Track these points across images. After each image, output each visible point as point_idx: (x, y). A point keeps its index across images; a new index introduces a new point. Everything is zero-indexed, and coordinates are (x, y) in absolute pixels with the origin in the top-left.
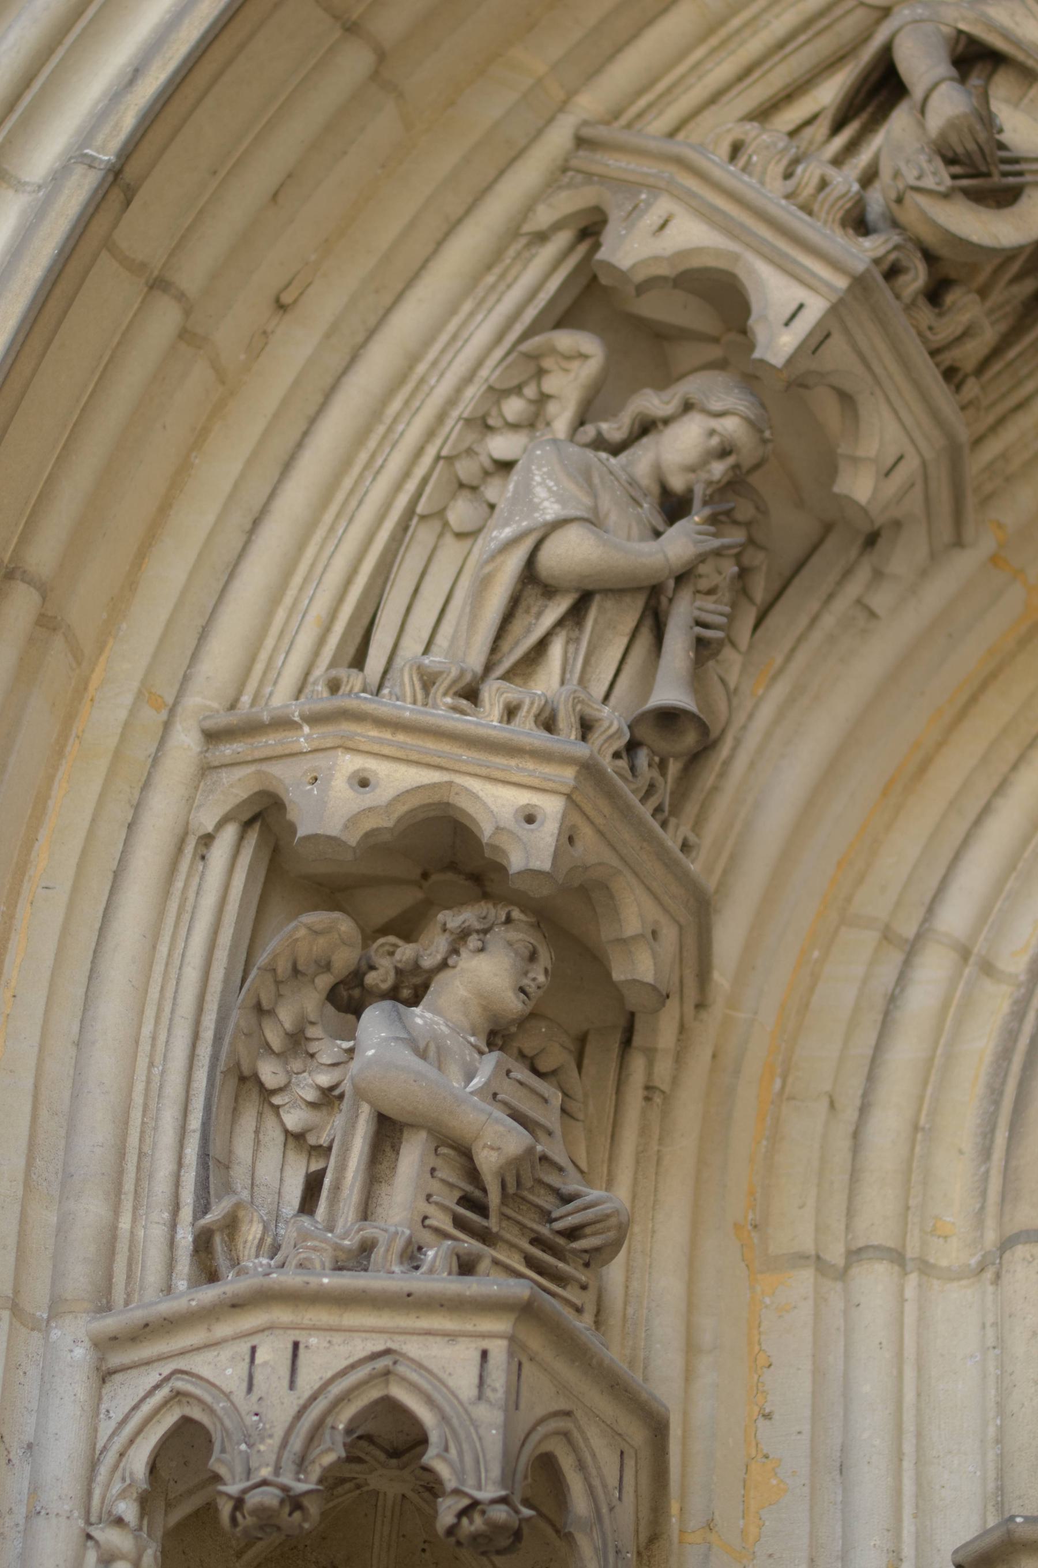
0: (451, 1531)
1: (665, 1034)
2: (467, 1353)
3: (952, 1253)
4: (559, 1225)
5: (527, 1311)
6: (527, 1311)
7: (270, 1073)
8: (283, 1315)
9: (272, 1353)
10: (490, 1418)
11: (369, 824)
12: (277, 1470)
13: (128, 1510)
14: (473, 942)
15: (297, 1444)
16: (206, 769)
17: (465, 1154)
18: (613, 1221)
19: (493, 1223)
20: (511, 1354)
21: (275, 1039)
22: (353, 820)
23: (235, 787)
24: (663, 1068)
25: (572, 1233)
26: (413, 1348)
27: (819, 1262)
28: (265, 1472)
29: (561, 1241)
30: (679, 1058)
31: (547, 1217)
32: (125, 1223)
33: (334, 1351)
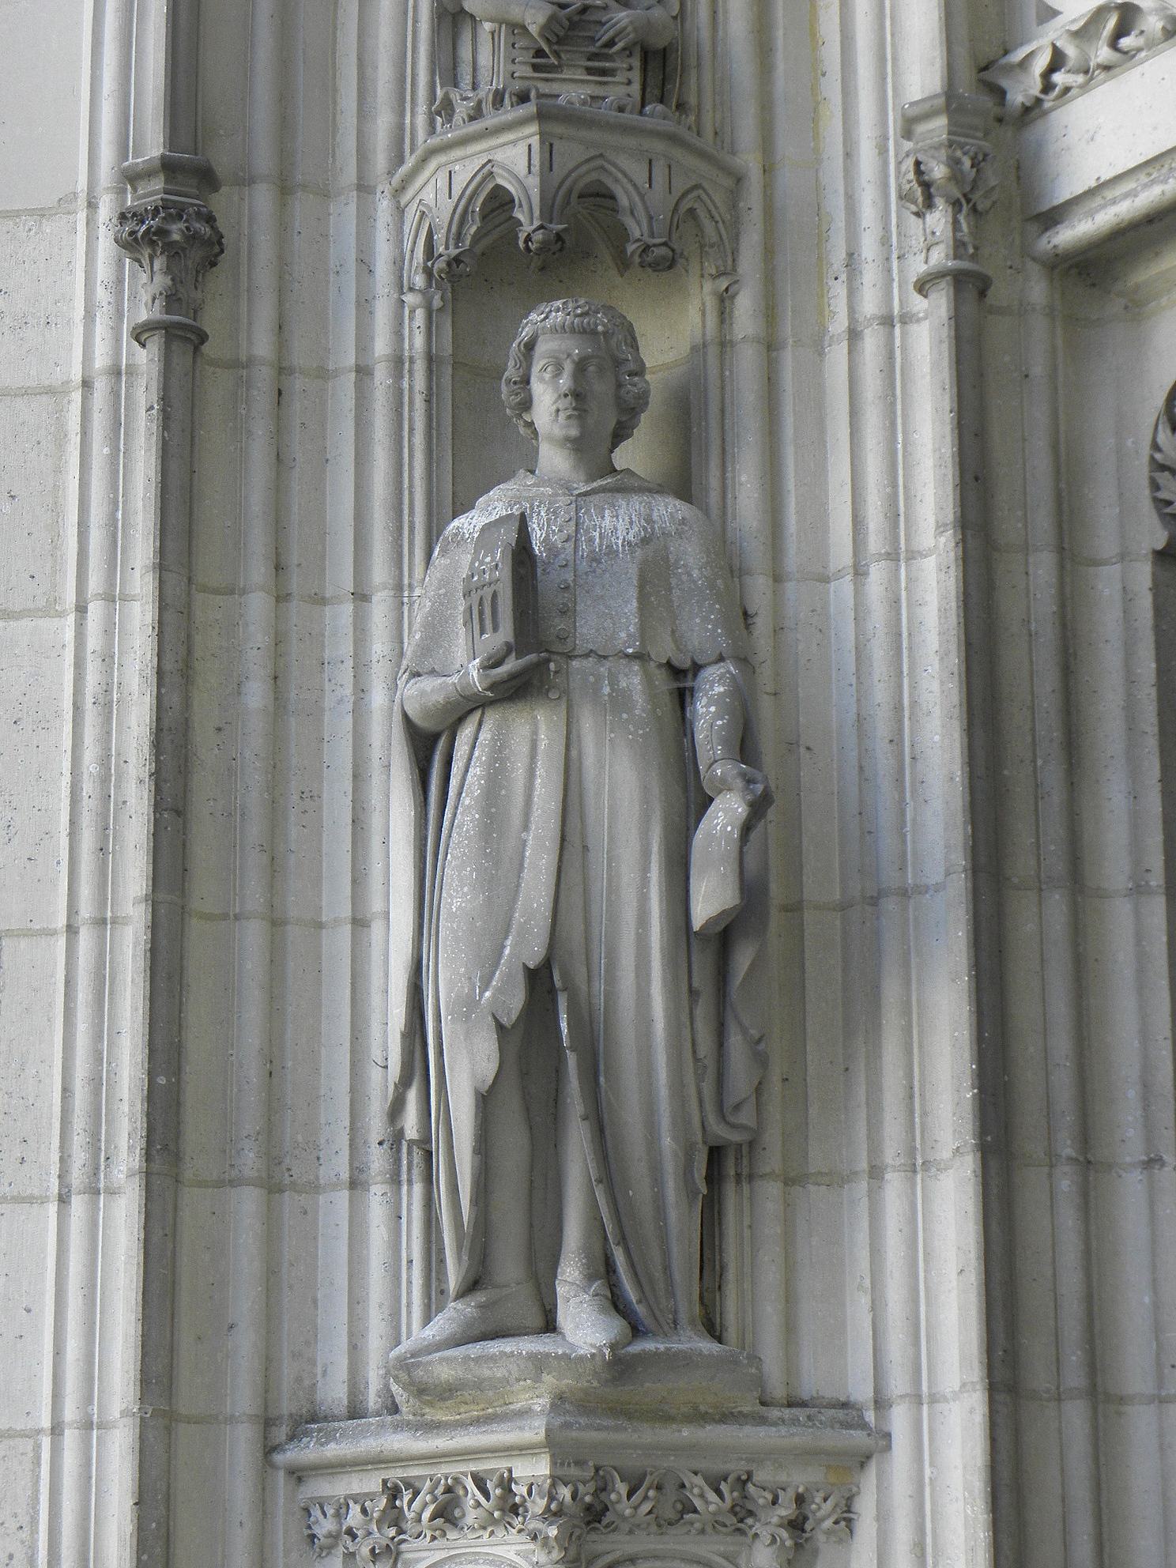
0: (528, 249)
2: (522, 149)
4: (599, 44)
8: (442, 159)
10: (533, 183)
12: (447, 248)
18: (630, 29)
19: (553, 60)
20: (542, 142)
29: (606, 51)
32: (408, 121)
33: (465, 169)
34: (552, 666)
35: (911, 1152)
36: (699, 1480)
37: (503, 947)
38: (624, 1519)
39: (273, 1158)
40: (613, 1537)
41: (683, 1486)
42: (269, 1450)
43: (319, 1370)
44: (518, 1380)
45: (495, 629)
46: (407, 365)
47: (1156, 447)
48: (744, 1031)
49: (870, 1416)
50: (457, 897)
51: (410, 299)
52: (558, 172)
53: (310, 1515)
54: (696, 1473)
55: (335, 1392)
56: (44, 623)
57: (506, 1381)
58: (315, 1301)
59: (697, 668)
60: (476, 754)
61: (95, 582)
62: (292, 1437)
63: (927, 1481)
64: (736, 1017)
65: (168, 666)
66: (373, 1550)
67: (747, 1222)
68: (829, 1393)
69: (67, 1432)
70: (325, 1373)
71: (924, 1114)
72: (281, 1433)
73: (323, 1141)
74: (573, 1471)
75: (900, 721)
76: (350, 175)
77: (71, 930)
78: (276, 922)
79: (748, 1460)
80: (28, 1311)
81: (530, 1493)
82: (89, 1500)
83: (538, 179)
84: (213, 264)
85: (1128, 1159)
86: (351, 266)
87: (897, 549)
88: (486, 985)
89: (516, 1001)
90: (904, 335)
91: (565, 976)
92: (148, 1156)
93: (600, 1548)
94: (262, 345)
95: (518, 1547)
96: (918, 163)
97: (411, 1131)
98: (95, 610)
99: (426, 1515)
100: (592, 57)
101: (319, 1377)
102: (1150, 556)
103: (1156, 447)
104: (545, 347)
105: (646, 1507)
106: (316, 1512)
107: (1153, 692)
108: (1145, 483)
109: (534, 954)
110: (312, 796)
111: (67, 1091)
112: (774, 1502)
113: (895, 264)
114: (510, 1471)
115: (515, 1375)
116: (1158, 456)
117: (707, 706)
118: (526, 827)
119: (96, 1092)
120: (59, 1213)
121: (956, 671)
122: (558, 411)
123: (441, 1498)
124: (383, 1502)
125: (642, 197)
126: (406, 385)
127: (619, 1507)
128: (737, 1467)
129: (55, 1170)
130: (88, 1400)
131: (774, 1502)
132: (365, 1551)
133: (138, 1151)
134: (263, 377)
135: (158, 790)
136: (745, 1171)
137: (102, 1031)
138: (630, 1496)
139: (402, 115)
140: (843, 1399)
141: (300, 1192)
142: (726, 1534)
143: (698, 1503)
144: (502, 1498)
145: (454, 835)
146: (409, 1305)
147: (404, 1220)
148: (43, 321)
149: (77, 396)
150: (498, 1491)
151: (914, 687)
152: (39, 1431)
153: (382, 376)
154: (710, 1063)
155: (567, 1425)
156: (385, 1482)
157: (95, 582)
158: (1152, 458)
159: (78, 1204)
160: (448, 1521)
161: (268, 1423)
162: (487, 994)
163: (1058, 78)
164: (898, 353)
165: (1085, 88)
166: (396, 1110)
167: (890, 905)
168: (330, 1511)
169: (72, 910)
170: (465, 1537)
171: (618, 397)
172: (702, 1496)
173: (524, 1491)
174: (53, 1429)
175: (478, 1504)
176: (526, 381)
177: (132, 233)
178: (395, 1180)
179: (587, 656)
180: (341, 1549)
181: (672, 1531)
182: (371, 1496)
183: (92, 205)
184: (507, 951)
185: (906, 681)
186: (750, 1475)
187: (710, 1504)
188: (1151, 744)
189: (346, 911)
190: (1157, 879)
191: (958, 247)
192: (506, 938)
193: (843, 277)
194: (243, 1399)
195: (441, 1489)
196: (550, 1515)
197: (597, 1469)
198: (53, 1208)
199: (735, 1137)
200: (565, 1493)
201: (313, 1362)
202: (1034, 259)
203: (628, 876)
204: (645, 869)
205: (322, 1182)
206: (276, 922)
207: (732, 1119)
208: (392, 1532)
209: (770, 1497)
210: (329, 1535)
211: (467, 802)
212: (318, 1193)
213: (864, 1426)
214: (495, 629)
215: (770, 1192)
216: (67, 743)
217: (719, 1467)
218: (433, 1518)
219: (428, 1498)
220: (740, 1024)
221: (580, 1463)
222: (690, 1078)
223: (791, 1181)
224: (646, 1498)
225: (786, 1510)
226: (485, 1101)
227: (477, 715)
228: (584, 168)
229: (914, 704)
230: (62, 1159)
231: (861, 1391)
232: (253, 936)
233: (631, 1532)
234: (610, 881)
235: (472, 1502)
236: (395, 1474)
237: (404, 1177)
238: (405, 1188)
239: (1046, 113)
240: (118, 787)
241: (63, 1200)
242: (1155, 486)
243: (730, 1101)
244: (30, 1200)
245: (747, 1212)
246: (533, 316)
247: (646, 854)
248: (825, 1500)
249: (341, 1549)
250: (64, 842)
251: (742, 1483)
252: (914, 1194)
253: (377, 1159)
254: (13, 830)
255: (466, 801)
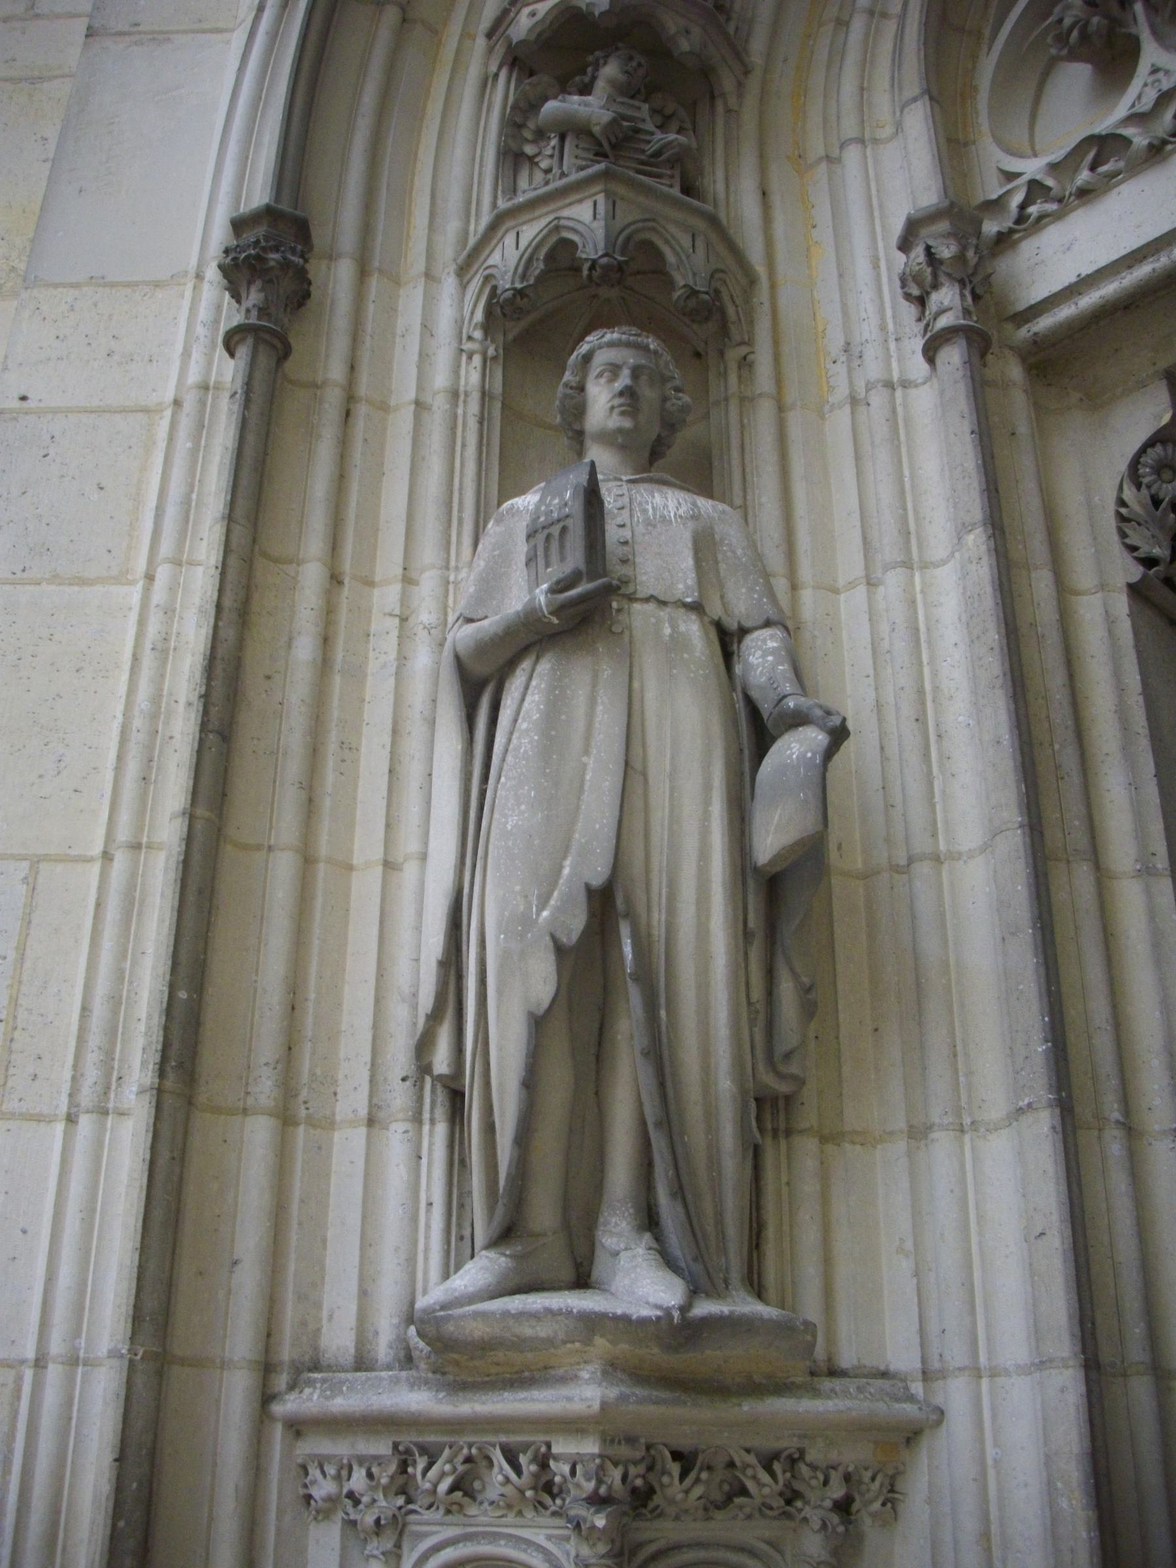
0: (590, 276)
1: (727, 83)
3: (888, 131)
5: (606, 175)
6: (606, 175)
7: (529, 150)
8: (509, 224)
9: (510, 240)
11: (538, 30)
12: (513, 283)
13: (478, 334)
14: (602, 61)
15: (520, 270)
16: (490, 50)
17: (590, 134)
20: (607, 197)
21: (528, 134)
22: (530, 30)
23: (500, 50)
24: (733, 102)
25: (658, 154)
26: (566, 213)
27: (828, 158)
28: (507, 286)
29: (652, 160)
30: (740, 96)
31: (643, 151)
34: (615, 605)
35: (958, 1111)
36: (751, 1459)
37: (561, 867)
38: (672, 1502)
39: (288, 1088)
40: (657, 1524)
41: (731, 1465)
42: (266, 1398)
43: (325, 1314)
44: (564, 1342)
45: (563, 559)
46: (462, 398)
47: (1122, 503)
48: (795, 975)
49: (917, 1388)
50: (512, 812)
51: (468, 346)
52: (619, 223)
53: (307, 1473)
54: (748, 1451)
55: (338, 1339)
56: (114, 589)
57: (550, 1342)
58: (324, 1241)
59: (743, 632)
60: (534, 683)
61: (166, 548)
62: (292, 1387)
63: (990, 1462)
64: (789, 962)
65: (227, 603)
66: (378, 1521)
67: (784, 1179)
68: (870, 1362)
69: (51, 1367)
70: (330, 1318)
71: (970, 1074)
72: (281, 1381)
73: (340, 1077)
74: (624, 1451)
75: (923, 703)
76: (420, 266)
77: (107, 856)
78: (308, 860)
79: (800, 1437)
80: (24, 1232)
81: (573, 1472)
82: (66, 1446)
83: (602, 223)
84: (301, 305)
85: (1157, 1127)
86: (417, 328)
87: (911, 559)
88: (543, 903)
89: (576, 924)
90: (905, 397)
91: (628, 901)
92: (162, 1073)
93: (647, 1535)
94: (336, 371)
95: (549, 1532)
96: (928, 249)
97: (441, 1062)
98: (163, 573)
99: (444, 1487)
100: (643, 163)
101: (324, 1322)
102: (1125, 589)
103: (1122, 503)
104: (601, 358)
105: (698, 1491)
106: (314, 1472)
107: (1141, 699)
108: (1114, 531)
109: (598, 874)
110: (349, 748)
111: (85, 1010)
112: (826, 1483)
113: (892, 345)
114: (549, 1446)
115: (561, 1335)
116: (1123, 511)
117: (763, 656)
118: (586, 752)
119: (115, 1012)
120: (65, 1133)
121: (996, 645)
122: (612, 408)
123: (461, 1469)
124: (393, 1468)
125: (688, 257)
126: (460, 411)
127: (669, 1492)
128: (789, 1444)
129: (66, 1088)
130: (77, 1333)
131: (826, 1483)
132: (369, 1519)
133: (151, 1067)
134: (333, 398)
135: (206, 712)
136: (782, 1126)
137: (126, 950)
138: (683, 1476)
139: (468, 222)
140: (882, 1368)
141: (314, 1127)
142: (775, 1518)
143: (750, 1485)
144: (536, 1476)
145: (509, 758)
146: (427, 1250)
147: (424, 1161)
148: (147, 358)
149: (168, 413)
150: (533, 1468)
151: (935, 674)
152: (23, 1362)
153: (440, 404)
154: (761, 1007)
155: (623, 1398)
156: (396, 1446)
157: (166, 548)
158: (1118, 514)
159: (85, 1123)
160: (466, 1494)
161: (267, 1368)
162: (545, 914)
163: (1033, 210)
164: (900, 410)
165: (1058, 216)
166: (423, 1046)
167: (923, 869)
168: (331, 1470)
169: (109, 837)
170: (485, 1513)
171: (663, 409)
172: (754, 1477)
173: (566, 1469)
174: (37, 1360)
175: (507, 1480)
176: (581, 388)
177: (234, 259)
178: (417, 1119)
179: (647, 600)
180: (340, 1515)
181: (719, 1515)
182: (378, 1459)
183: (199, 276)
184: (566, 871)
185: (926, 671)
186: (802, 1452)
187: (764, 1486)
188: (1143, 743)
189: (378, 853)
190: (1162, 862)
191: (966, 312)
192: (565, 858)
193: (843, 359)
194: (241, 1342)
195: (460, 1458)
196: (597, 1501)
197: (648, 1447)
198: (60, 1127)
199: (783, 1088)
200: (616, 1474)
201: (318, 1305)
202: (1011, 348)
203: (690, 808)
204: (707, 802)
205: (338, 1118)
206: (308, 860)
207: (782, 1068)
208: (400, 1501)
209: (821, 1477)
210: (329, 1499)
211: (525, 726)
212: (333, 1129)
213: (911, 1398)
214: (563, 559)
215: (807, 1146)
216: (123, 689)
217: (769, 1444)
218: (453, 1489)
219: (447, 1467)
220: (792, 970)
221: (631, 1440)
222: (744, 1022)
223: (830, 1137)
224: (698, 1480)
225: (837, 1491)
226: (538, 1023)
227: (526, 664)
228: (641, 225)
229: (936, 689)
230: (74, 1078)
231: (902, 1357)
232: (283, 869)
233: (677, 1518)
234: (672, 811)
235: (500, 1478)
236: (408, 1439)
237: (426, 1116)
238: (426, 1128)
239: (1014, 245)
240: (167, 723)
241: (71, 1119)
242: (1123, 535)
243: (781, 1049)
244: (39, 1118)
245: (784, 1166)
246: (588, 339)
247: (707, 787)
248: (873, 1479)
249: (340, 1515)
250: (109, 776)
251: (792, 1462)
252: (962, 1153)
253: (399, 1096)
254: (62, 764)
255: (523, 725)
